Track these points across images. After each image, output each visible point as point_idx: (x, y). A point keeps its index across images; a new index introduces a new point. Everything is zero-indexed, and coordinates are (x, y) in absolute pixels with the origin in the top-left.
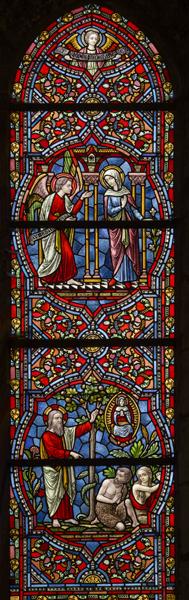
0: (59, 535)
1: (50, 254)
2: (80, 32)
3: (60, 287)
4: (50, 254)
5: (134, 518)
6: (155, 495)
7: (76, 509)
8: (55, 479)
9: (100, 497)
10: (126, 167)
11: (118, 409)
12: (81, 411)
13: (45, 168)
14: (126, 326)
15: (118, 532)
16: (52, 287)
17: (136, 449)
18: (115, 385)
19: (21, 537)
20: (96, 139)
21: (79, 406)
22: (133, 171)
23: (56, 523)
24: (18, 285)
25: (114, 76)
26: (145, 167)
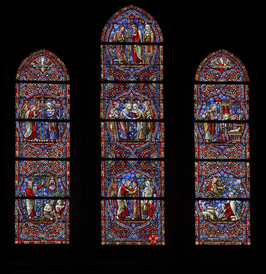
0: (31, 222)
1: (28, 130)
2: (39, 58)
3: (32, 141)
4: (28, 130)
5: (56, 216)
6: (63, 209)
7: (37, 213)
8: (30, 204)
9: (45, 209)
10: (54, 102)
11: (51, 181)
12: (39, 181)
13: (27, 102)
14: (54, 154)
15: (51, 221)
16: (29, 141)
17: (57, 194)
18: (50, 173)
19: (19, 222)
20: (44, 93)
21: (38, 180)
22: (57, 103)
23: (30, 217)
24: (18, 140)
25: (50, 72)
26: (60, 102)
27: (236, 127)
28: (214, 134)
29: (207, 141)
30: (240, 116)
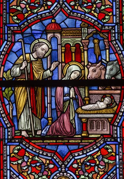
27: (99, 97)
28: (43, 116)
29: (24, 133)
30: (109, 68)
